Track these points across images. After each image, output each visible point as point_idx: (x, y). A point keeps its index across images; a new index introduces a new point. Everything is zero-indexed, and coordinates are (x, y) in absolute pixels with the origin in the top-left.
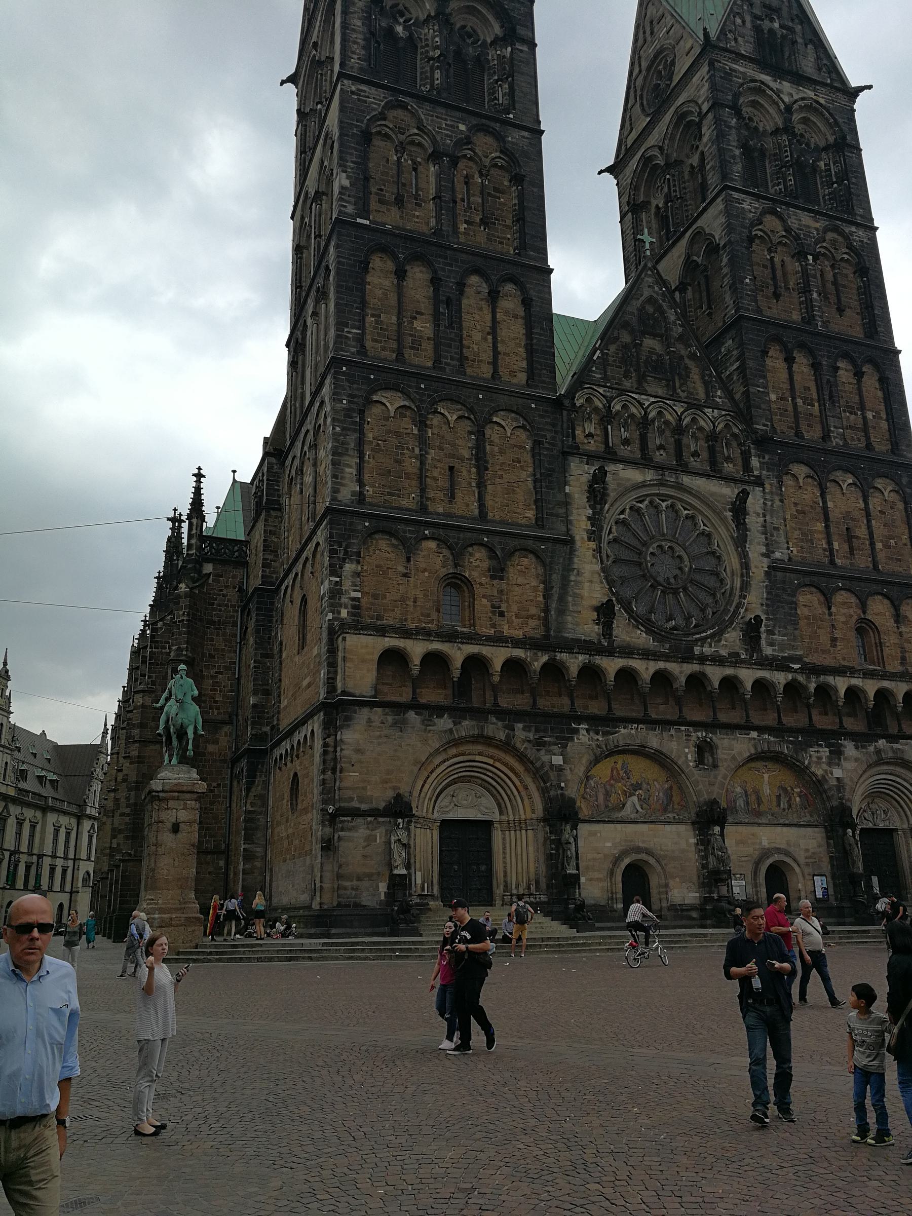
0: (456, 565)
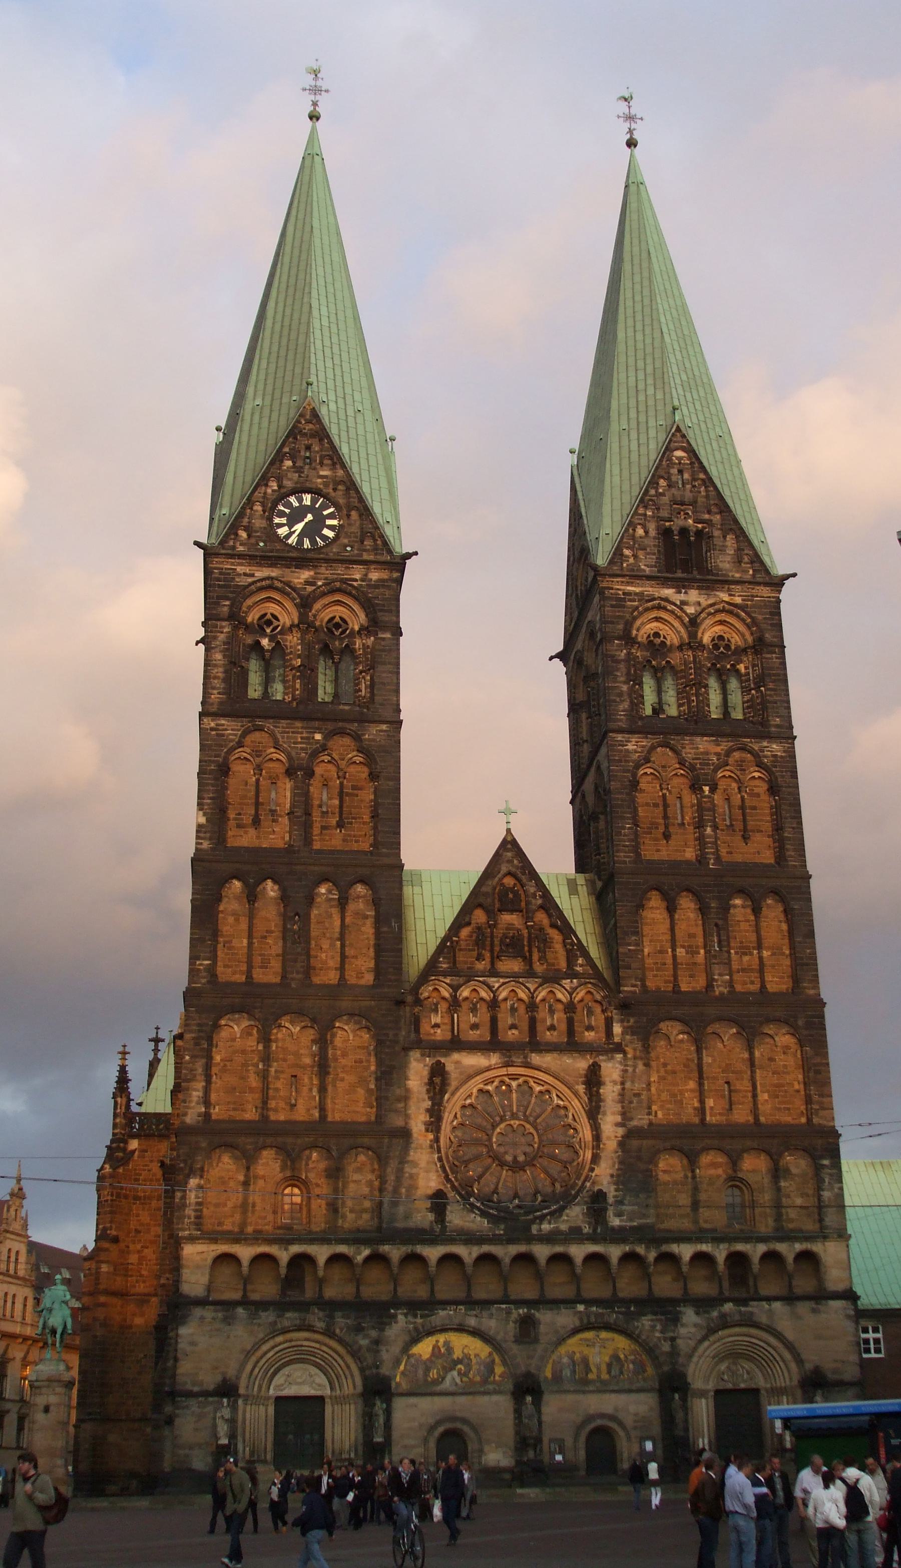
0: (293, 1170)
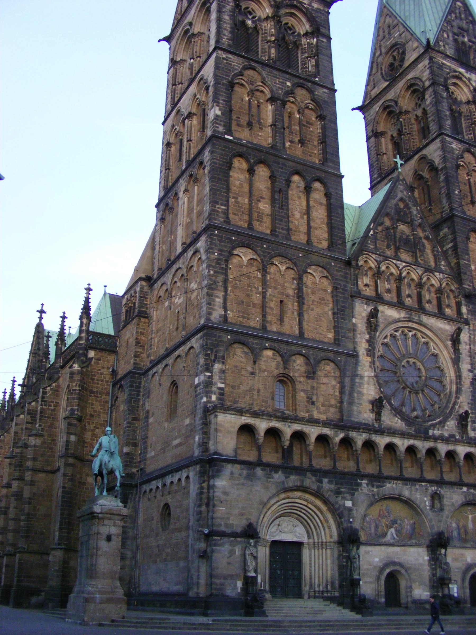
0: (285, 368)
